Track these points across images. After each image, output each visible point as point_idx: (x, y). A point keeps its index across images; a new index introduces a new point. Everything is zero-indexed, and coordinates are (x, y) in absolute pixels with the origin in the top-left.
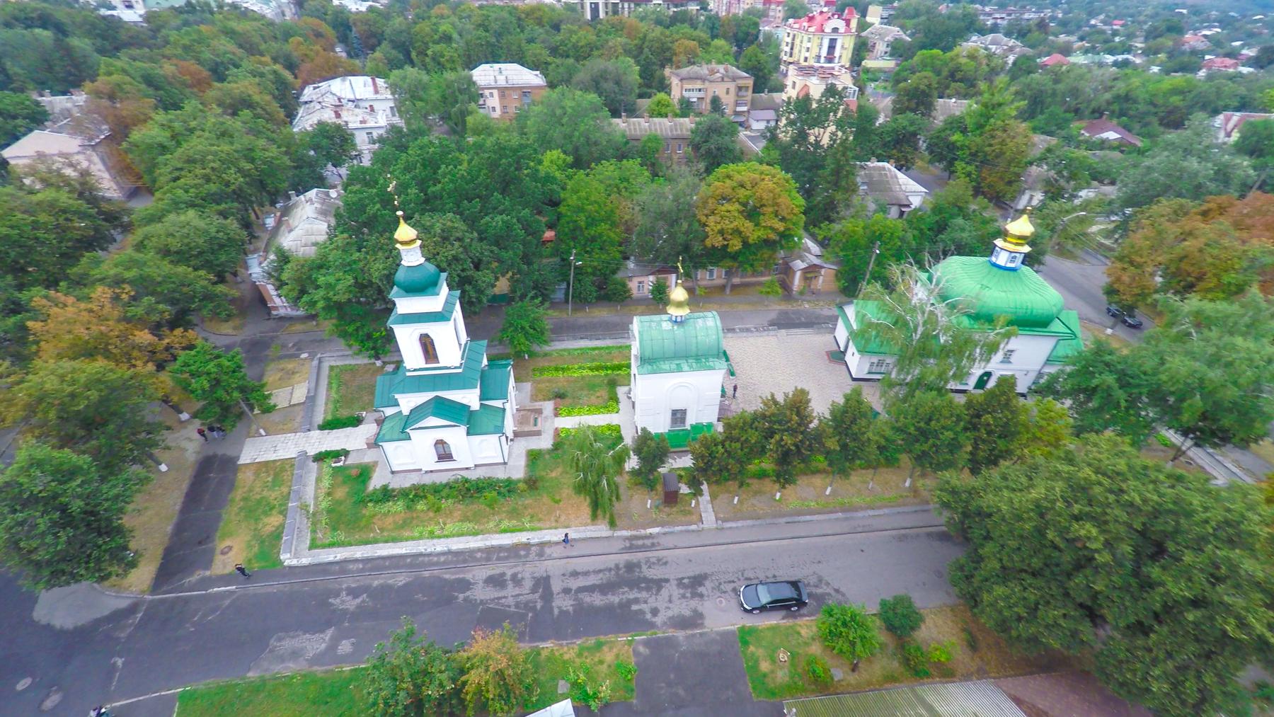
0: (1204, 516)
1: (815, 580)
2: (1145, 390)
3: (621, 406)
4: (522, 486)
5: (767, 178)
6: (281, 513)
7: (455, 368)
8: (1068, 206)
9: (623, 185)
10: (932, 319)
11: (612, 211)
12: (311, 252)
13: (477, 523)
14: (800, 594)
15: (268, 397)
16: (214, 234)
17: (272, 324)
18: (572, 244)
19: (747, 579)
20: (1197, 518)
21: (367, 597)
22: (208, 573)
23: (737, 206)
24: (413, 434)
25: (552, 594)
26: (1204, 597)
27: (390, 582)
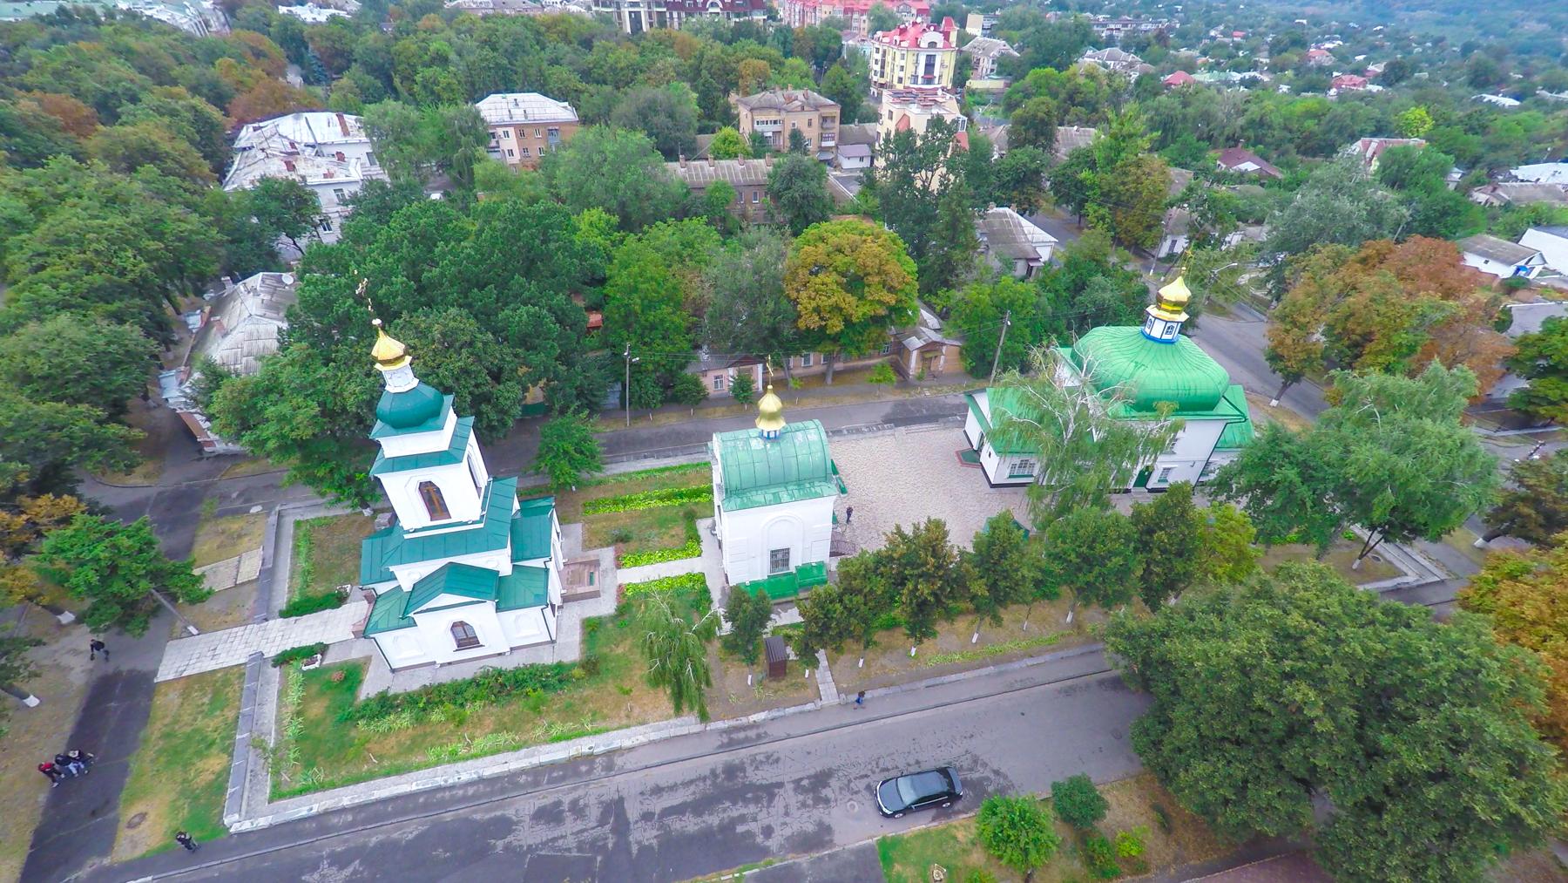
0: (1435, 665)
1: (969, 761)
2: (1332, 486)
3: (704, 546)
4: (577, 672)
5: (869, 239)
6: (224, 750)
7: (474, 523)
8: (1216, 254)
9: (686, 253)
10: (1082, 415)
11: (674, 288)
12: (258, 372)
13: (517, 732)
14: (951, 784)
15: (199, 579)
16: (101, 349)
17: (204, 465)
18: (625, 334)
19: (883, 770)
20: (1427, 668)
21: (360, 865)
22: (107, 861)
23: (835, 276)
24: (417, 618)
25: (628, 823)
26: (1444, 767)
27: (395, 835)
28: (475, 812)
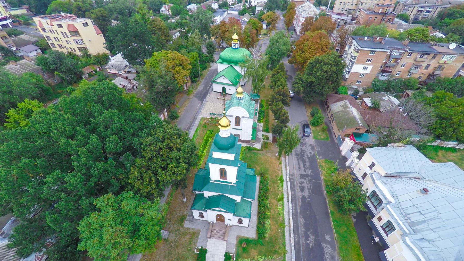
21: (309, 232)
27: (302, 224)
28: (299, 205)
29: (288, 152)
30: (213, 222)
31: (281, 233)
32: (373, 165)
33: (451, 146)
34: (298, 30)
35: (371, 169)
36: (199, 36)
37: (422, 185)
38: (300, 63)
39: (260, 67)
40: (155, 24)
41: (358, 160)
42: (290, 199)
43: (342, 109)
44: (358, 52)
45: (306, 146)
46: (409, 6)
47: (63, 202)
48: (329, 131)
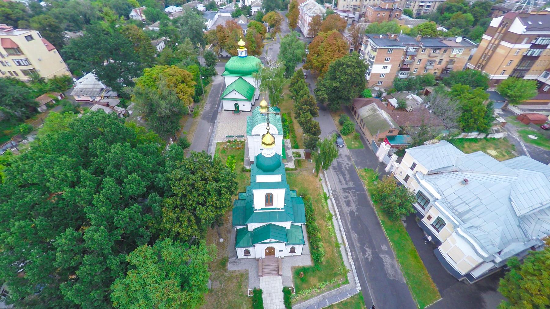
21: (365, 246)
27: (356, 239)
29: (326, 167)
30: (262, 258)
31: (337, 254)
32: (414, 165)
33: (473, 137)
34: (305, 31)
35: (413, 170)
36: (191, 45)
37: (462, 177)
38: (317, 68)
39: (277, 75)
40: (130, 33)
41: (398, 164)
42: (339, 217)
43: (371, 113)
44: (376, 51)
45: (341, 158)
46: (411, 1)
47: (87, 267)
48: (361, 138)
